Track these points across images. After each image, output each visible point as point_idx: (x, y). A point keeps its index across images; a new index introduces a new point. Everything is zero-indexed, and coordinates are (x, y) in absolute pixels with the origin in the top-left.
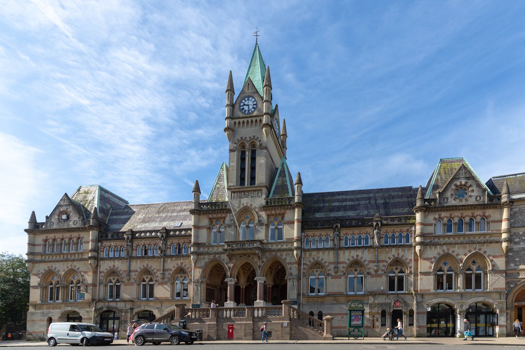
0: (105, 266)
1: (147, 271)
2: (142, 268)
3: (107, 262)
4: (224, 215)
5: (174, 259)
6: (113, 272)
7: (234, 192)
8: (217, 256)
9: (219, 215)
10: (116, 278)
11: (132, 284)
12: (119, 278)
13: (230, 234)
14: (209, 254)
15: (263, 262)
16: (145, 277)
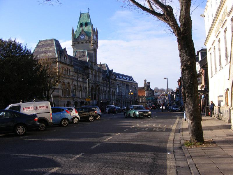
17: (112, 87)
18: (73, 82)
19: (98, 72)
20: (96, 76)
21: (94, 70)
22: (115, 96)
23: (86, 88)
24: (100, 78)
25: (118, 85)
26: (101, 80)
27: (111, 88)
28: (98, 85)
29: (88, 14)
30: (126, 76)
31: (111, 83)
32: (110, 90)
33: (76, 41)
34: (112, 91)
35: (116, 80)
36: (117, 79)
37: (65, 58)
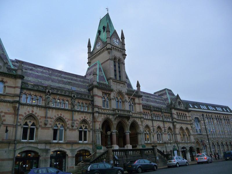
0: (24, 111)
2: (57, 116)
3: (26, 107)
4: (110, 92)
5: (80, 113)
6: (31, 116)
7: (114, 81)
8: (108, 116)
9: (108, 92)
10: (32, 122)
11: (48, 128)
12: (35, 123)
13: (114, 105)
14: (105, 114)
15: (129, 122)
16: (58, 123)
18: (16, 110)
19: (127, 94)
20: (122, 101)
21: (112, 90)
22: (192, 137)
23: (84, 121)
24: (137, 106)
25: (197, 118)
26: (139, 108)
27: (175, 124)
28: (128, 118)
29: (107, 16)
30: (214, 106)
31: (175, 116)
32: (174, 126)
33: (92, 55)
34: (181, 128)
35: (190, 111)
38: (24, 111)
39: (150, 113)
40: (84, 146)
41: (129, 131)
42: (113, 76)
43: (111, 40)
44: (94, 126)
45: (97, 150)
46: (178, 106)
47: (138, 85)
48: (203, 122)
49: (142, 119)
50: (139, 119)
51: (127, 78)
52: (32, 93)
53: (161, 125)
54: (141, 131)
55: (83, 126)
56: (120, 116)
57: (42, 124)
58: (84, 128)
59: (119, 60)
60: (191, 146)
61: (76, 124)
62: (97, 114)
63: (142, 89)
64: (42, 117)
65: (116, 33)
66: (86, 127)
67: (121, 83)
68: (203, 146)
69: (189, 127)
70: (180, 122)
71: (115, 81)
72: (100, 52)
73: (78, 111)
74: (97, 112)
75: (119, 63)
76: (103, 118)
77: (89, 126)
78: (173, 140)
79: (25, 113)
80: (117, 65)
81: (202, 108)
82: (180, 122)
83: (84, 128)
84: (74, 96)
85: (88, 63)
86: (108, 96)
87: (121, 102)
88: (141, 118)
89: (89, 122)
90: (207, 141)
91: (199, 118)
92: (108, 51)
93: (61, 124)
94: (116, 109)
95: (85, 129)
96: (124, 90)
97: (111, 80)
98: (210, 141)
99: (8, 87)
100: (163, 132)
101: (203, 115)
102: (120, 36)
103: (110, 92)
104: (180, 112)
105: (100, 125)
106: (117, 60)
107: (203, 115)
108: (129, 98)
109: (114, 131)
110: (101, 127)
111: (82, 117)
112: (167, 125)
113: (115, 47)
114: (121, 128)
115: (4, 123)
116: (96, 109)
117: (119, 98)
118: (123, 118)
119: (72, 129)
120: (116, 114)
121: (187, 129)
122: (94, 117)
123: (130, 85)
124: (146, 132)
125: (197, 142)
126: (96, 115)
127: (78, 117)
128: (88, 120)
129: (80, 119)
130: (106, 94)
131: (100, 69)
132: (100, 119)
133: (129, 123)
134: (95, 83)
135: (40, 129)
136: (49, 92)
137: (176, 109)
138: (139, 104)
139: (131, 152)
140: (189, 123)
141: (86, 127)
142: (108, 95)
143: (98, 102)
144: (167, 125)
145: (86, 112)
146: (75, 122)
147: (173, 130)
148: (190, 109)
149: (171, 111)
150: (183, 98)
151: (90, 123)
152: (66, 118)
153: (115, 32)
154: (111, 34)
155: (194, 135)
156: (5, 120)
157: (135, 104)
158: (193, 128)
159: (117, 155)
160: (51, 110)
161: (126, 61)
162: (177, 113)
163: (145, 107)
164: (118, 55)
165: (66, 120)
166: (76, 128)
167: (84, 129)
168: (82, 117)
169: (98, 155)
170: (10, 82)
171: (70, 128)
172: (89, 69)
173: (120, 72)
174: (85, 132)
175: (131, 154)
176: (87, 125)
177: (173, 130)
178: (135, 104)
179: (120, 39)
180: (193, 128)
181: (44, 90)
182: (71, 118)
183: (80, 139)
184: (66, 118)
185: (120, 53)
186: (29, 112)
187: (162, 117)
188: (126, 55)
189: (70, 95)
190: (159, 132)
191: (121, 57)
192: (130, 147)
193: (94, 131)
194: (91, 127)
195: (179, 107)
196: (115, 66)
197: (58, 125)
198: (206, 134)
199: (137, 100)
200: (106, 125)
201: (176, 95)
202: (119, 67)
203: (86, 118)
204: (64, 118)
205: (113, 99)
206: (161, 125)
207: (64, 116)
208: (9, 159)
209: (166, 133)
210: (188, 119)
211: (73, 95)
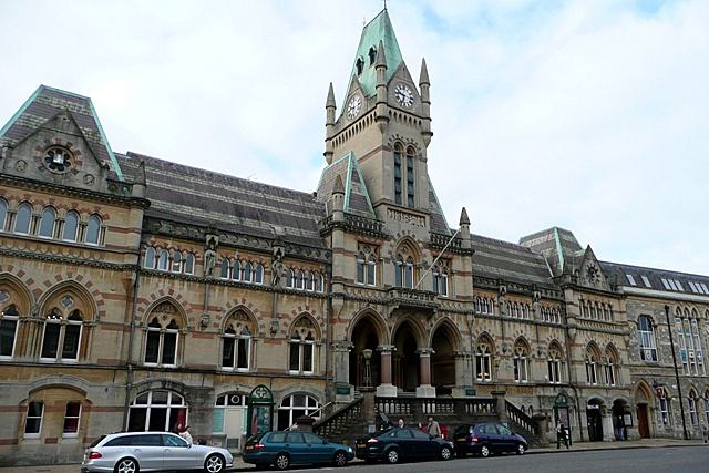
0: (150, 290)
1: (241, 313)
4: (378, 242)
5: (294, 297)
8: (371, 306)
12: (178, 319)
13: (388, 274)
14: (360, 300)
16: (234, 323)
17: (579, 325)
18: (132, 288)
21: (386, 237)
23: (305, 319)
26: (462, 286)
28: (428, 312)
32: (570, 341)
33: (338, 132)
34: (592, 345)
35: (626, 295)
36: (626, 289)
37: (59, 159)
38: (150, 290)
39: (496, 299)
40: (302, 382)
41: (431, 349)
42: (390, 197)
43: (390, 92)
44: (330, 332)
45: (338, 396)
46: (587, 281)
47: (464, 221)
48: (664, 329)
49: (470, 318)
50: (462, 317)
51: (432, 196)
52: (170, 243)
53: (529, 333)
54: (464, 349)
55: (303, 331)
56: (404, 308)
57: (195, 325)
58: (303, 336)
59: (410, 150)
60: (620, 397)
61: (284, 327)
62: (341, 302)
63: (474, 230)
64: (194, 306)
65: (405, 69)
66: (310, 333)
67: (412, 215)
68: (658, 400)
69: (619, 343)
70: (589, 326)
71: (396, 208)
72: (358, 125)
73: (290, 293)
74: (339, 295)
75: (407, 155)
76: (356, 311)
77: (319, 335)
78: (563, 378)
79: (153, 296)
80: (404, 162)
81: (668, 287)
82: (589, 326)
83: (303, 336)
84: (279, 252)
85: (325, 154)
86: (373, 252)
87: (410, 268)
88: (466, 314)
89: (319, 322)
90: (675, 387)
91: (654, 318)
92: (379, 123)
93: (243, 326)
94: (393, 289)
95: (168, 327)
96: (422, 233)
97: (383, 208)
98: (683, 387)
99: (111, 229)
100: (533, 356)
101: (667, 308)
102: (416, 80)
103: (378, 242)
104: (592, 297)
105: (347, 330)
106: (405, 148)
107: (667, 308)
108: (435, 257)
109: (386, 346)
110: (350, 337)
111: (300, 308)
112: (548, 335)
113: (398, 113)
114: (406, 337)
115: (102, 319)
116: (337, 288)
117: (405, 257)
118: (412, 313)
119: (272, 339)
120: (393, 302)
121: (611, 347)
122: (331, 309)
123: (437, 220)
124: (481, 352)
125: (641, 387)
126: (337, 302)
127: (289, 308)
128: (315, 317)
129: (294, 313)
130: (368, 245)
131: (354, 172)
132: (350, 314)
133: (430, 327)
134: (337, 217)
135: (189, 337)
136: (212, 241)
137: (576, 288)
138: (463, 274)
139: (434, 405)
140: (619, 330)
141: (310, 333)
142: (373, 249)
143: (345, 266)
144: (548, 335)
145: (310, 295)
146: (281, 322)
147: (565, 350)
148: (626, 289)
149: (563, 295)
150: (602, 255)
151: (322, 325)
152: (256, 311)
153: (403, 68)
154: (389, 73)
155: (632, 367)
156: (103, 313)
157: (452, 273)
158: (632, 347)
159: (387, 410)
160: (217, 288)
161: (433, 152)
162: (582, 301)
163: (480, 280)
164: (407, 132)
165: (258, 315)
166: (284, 337)
167: (164, 327)
168: (300, 308)
169: (337, 408)
170: (115, 216)
171: (268, 335)
172: (326, 172)
173: (410, 183)
174: (308, 349)
175: (434, 411)
176: (312, 330)
177: (565, 350)
178: (452, 273)
179: (417, 85)
180: (632, 347)
181: (201, 237)
182: (270, 311)
183: (294, 365)
184: (256, 311)
185: (414, 130)
186: (161, 292)
187: (534, 311)
188: (432, 134)
189: (269, 249)
190: (520, 354)
191: (418, 140)
192: (427, 391)
193: (330, 345)
194: (324, 336)
195: (588, 285)
196: (397, 165)
197: (235, 328)
198: (673, 365)
199: (457, 264)
200: (365, 330)
201: (585, 248)
202: (410, 169)
203: (310, 312)
204: (252, 310)
205: (387, 260)
206: (529, 333)
207: (251, 305)
208: (117, 409)
209: (542, 356)
210: (617, 317)
211: (276, 249)
